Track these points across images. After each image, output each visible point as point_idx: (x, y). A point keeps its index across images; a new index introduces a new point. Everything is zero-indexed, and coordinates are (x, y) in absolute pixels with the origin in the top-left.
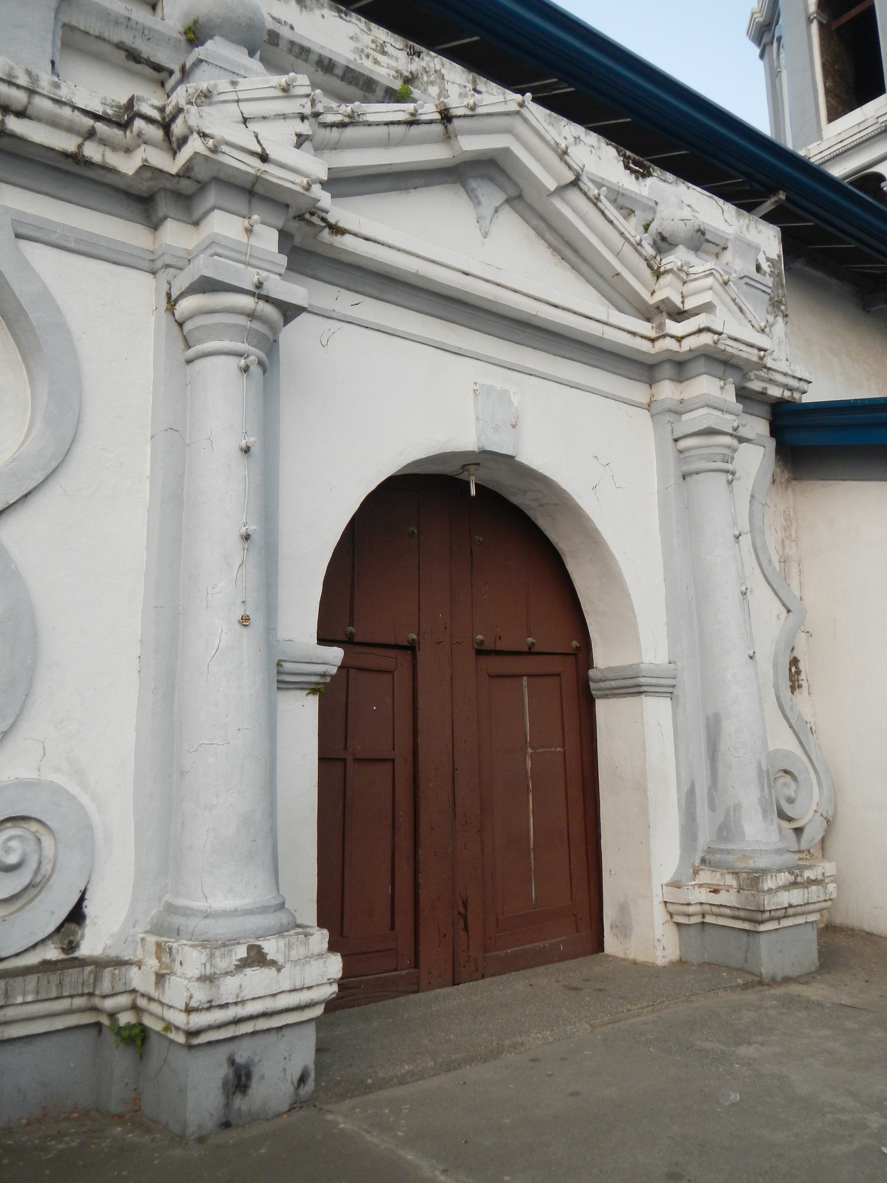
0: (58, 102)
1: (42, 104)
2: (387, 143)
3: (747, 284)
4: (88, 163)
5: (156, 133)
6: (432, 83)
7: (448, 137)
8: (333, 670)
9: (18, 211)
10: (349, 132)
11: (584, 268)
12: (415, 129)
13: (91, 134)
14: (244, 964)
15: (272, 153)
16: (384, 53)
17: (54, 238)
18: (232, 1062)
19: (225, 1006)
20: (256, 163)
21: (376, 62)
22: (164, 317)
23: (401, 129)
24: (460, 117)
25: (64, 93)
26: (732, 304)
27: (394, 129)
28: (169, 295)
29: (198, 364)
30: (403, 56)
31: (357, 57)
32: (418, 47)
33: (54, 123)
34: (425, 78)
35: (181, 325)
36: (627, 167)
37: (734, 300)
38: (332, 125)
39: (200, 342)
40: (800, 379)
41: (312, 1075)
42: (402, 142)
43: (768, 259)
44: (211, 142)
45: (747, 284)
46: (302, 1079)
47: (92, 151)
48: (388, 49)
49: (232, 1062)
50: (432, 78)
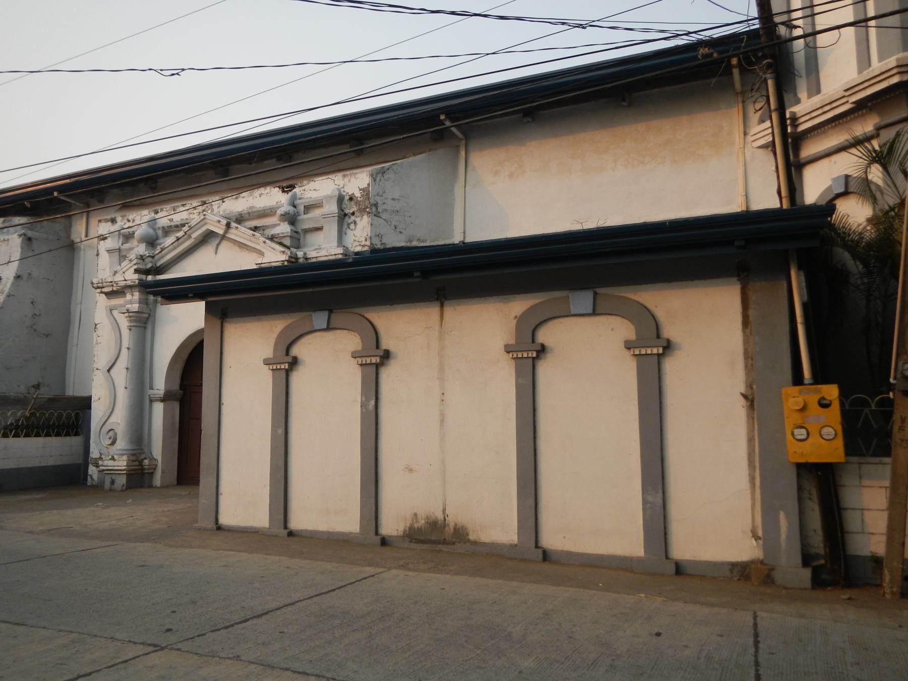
0: (106, 283)
1: (104, 284)
2: (175, 248)
3: (323, 218)
4: (115, 291)
7: (190, 237)
8: (162, 396)
10: (163, 252)
11: (249, 248)
12: (180, 241)
14: (111, 459)
15: (127, 279)
18: (112, 478)
19: (105, 466)
20: (125, 282)
21: (194, 213)
23: (176, 243)
24: (187, 231)
25: (106, 281)
26: (269, 248)
27: (174, 244)
36: (283, 191)
37: (270, 247)
38: (158, 253)
40: (335, 255)
41: (125, 485)
42: (179, 246)
43: (360, 190)
45: (323, 218)
46: (123, 486)
49: (112, 478)
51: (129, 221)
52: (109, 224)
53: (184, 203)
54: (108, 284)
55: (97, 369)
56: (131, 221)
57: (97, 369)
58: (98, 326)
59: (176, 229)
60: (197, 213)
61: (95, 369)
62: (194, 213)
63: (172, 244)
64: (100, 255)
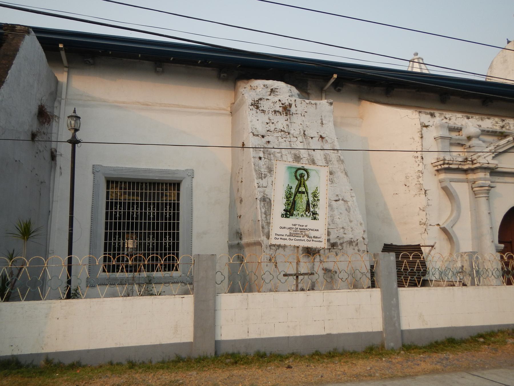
0: (456, 161)
5: (471, 162)
6: (507, 126)
9: (451, 178)
13: (460, 164)
15: (490, 163)
16: (497, 123)
17: (454, 181)
21: (496, 126)
22: (471, 191)
25: (457, 160)
28: (472, 187)
29: (478, 199)
30: (501, 122)
31: (492, 126)
32: (504, 119)
33: (456, 164)
34: (506, 125)
35: (474, 191)
39: (478, 195)
44: (481, 164)
47: (460, 167)
48: (498, 122)
50: (507, 125)
51: (446, 118)
52: (429, 116)
53: (489, 117)
54: (457, 162)
55: (430, 225)
56: (448, 119)
57: (430, 225)
58: (427, 192)
59: (487, 133)
60: (499, 126)
61: (428, 225)
62: (496, 126)
63: (503, 144)
64: (424, 138)
